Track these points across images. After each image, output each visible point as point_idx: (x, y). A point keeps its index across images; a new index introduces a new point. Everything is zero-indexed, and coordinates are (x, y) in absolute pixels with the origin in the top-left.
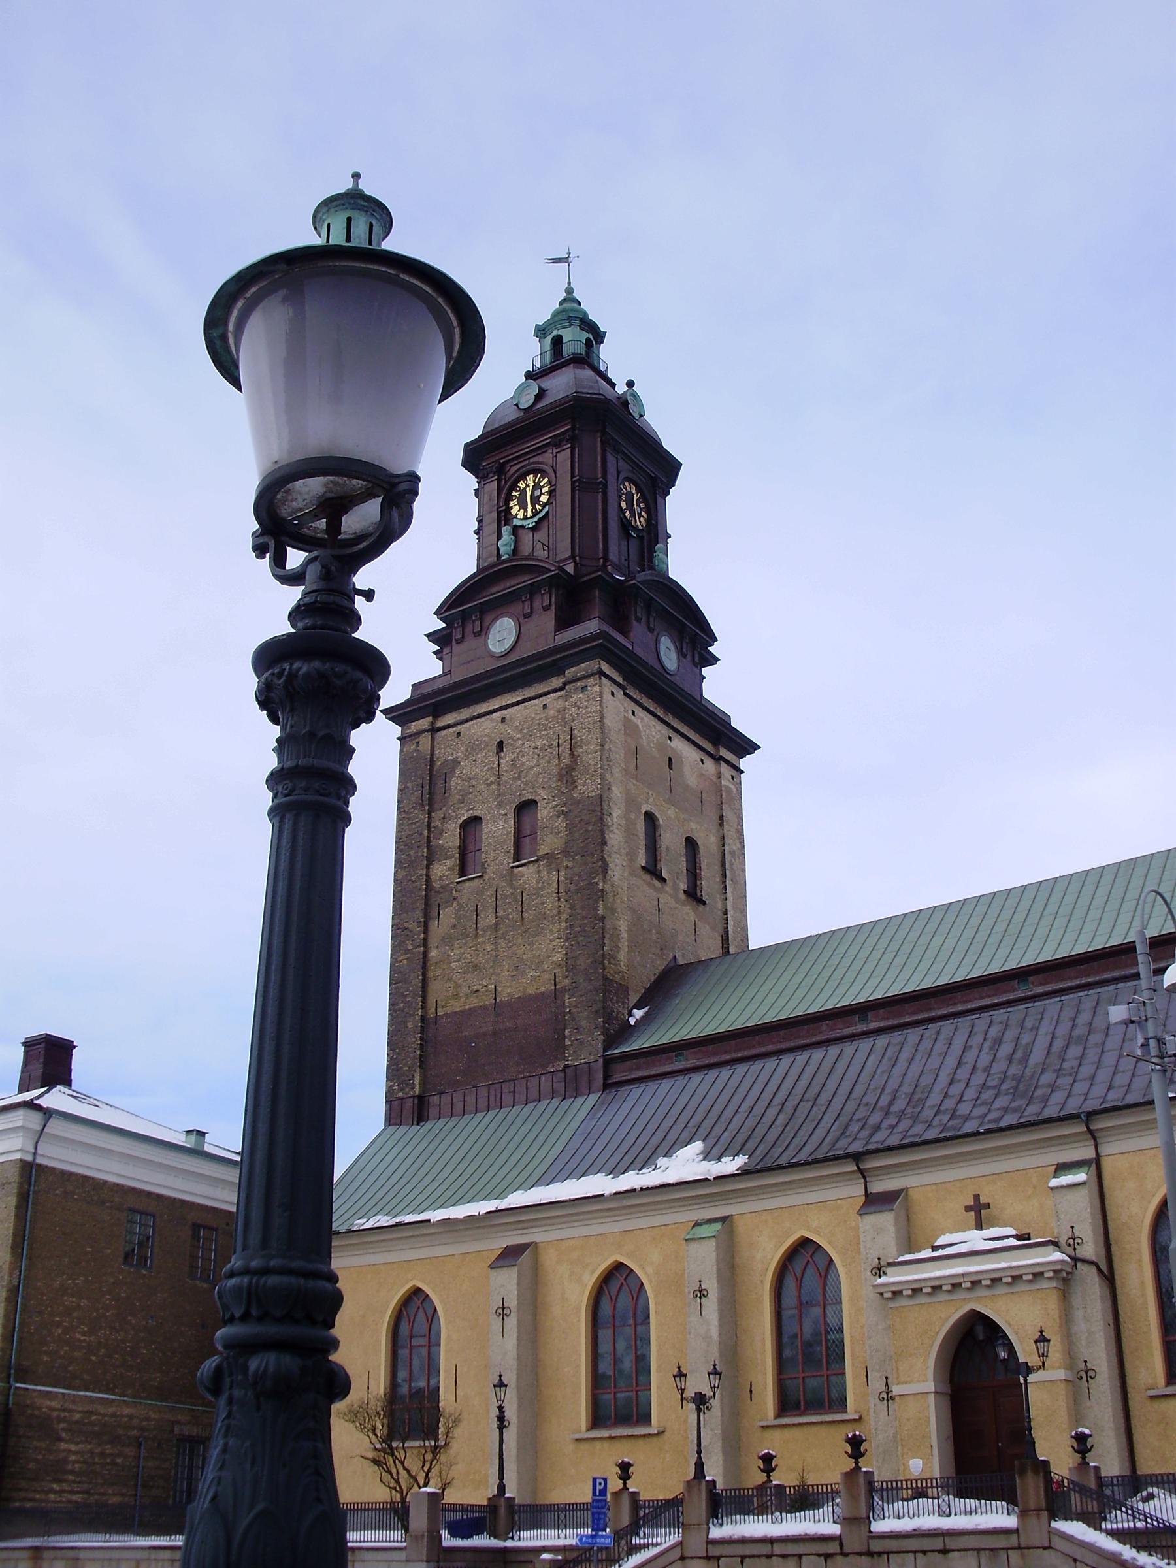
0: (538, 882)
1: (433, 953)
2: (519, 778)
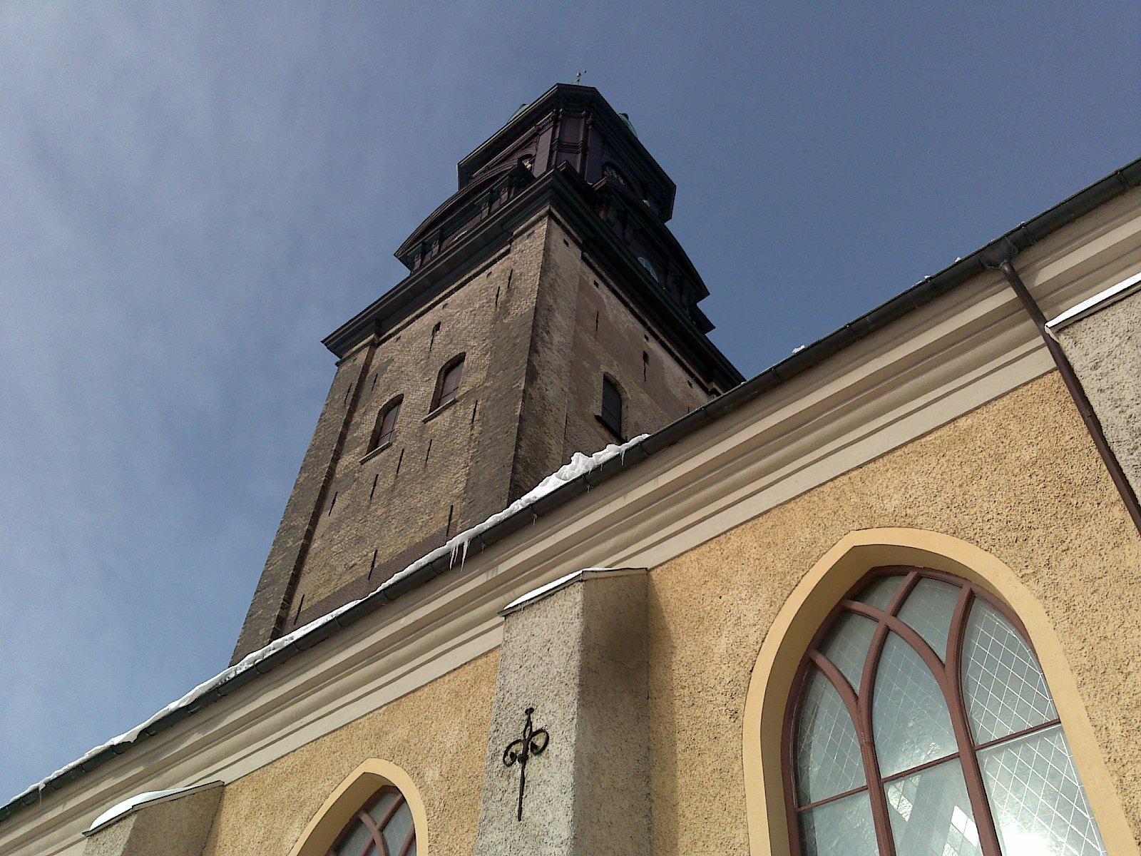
1: (316, 545)
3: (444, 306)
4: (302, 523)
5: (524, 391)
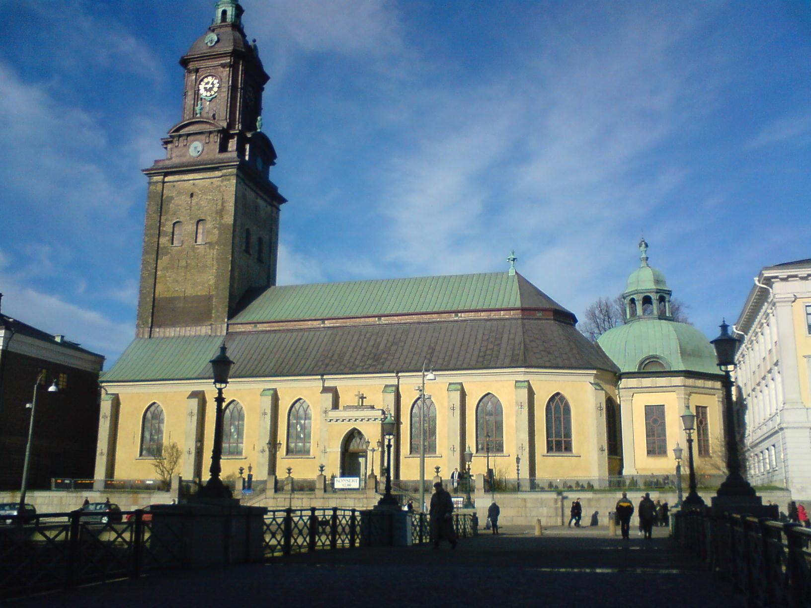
0: (205, 252)
1: (158, 273)
2: (199, 210)
4: (152, 262)
5: (232, 261)
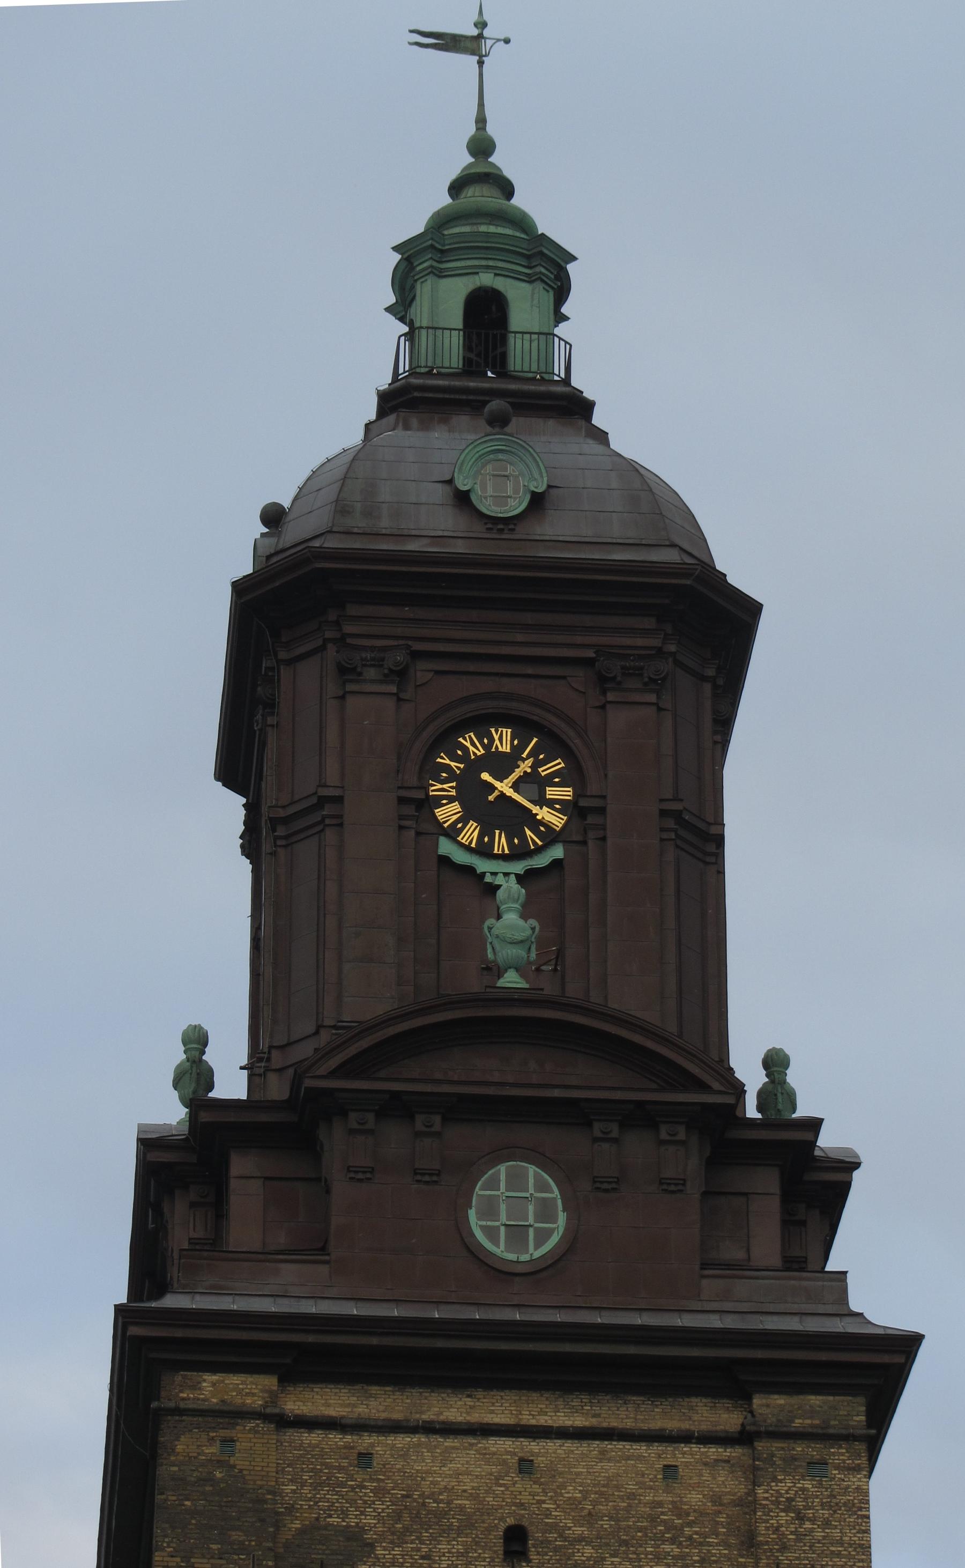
3: (525, 1466)
